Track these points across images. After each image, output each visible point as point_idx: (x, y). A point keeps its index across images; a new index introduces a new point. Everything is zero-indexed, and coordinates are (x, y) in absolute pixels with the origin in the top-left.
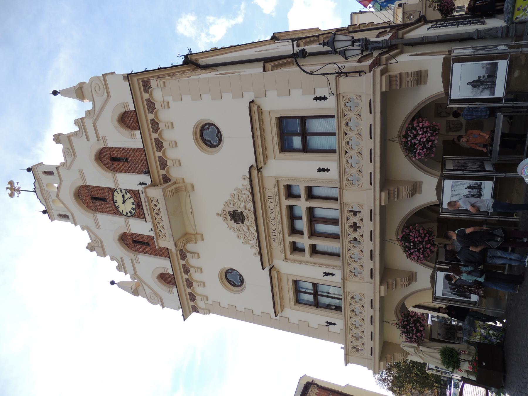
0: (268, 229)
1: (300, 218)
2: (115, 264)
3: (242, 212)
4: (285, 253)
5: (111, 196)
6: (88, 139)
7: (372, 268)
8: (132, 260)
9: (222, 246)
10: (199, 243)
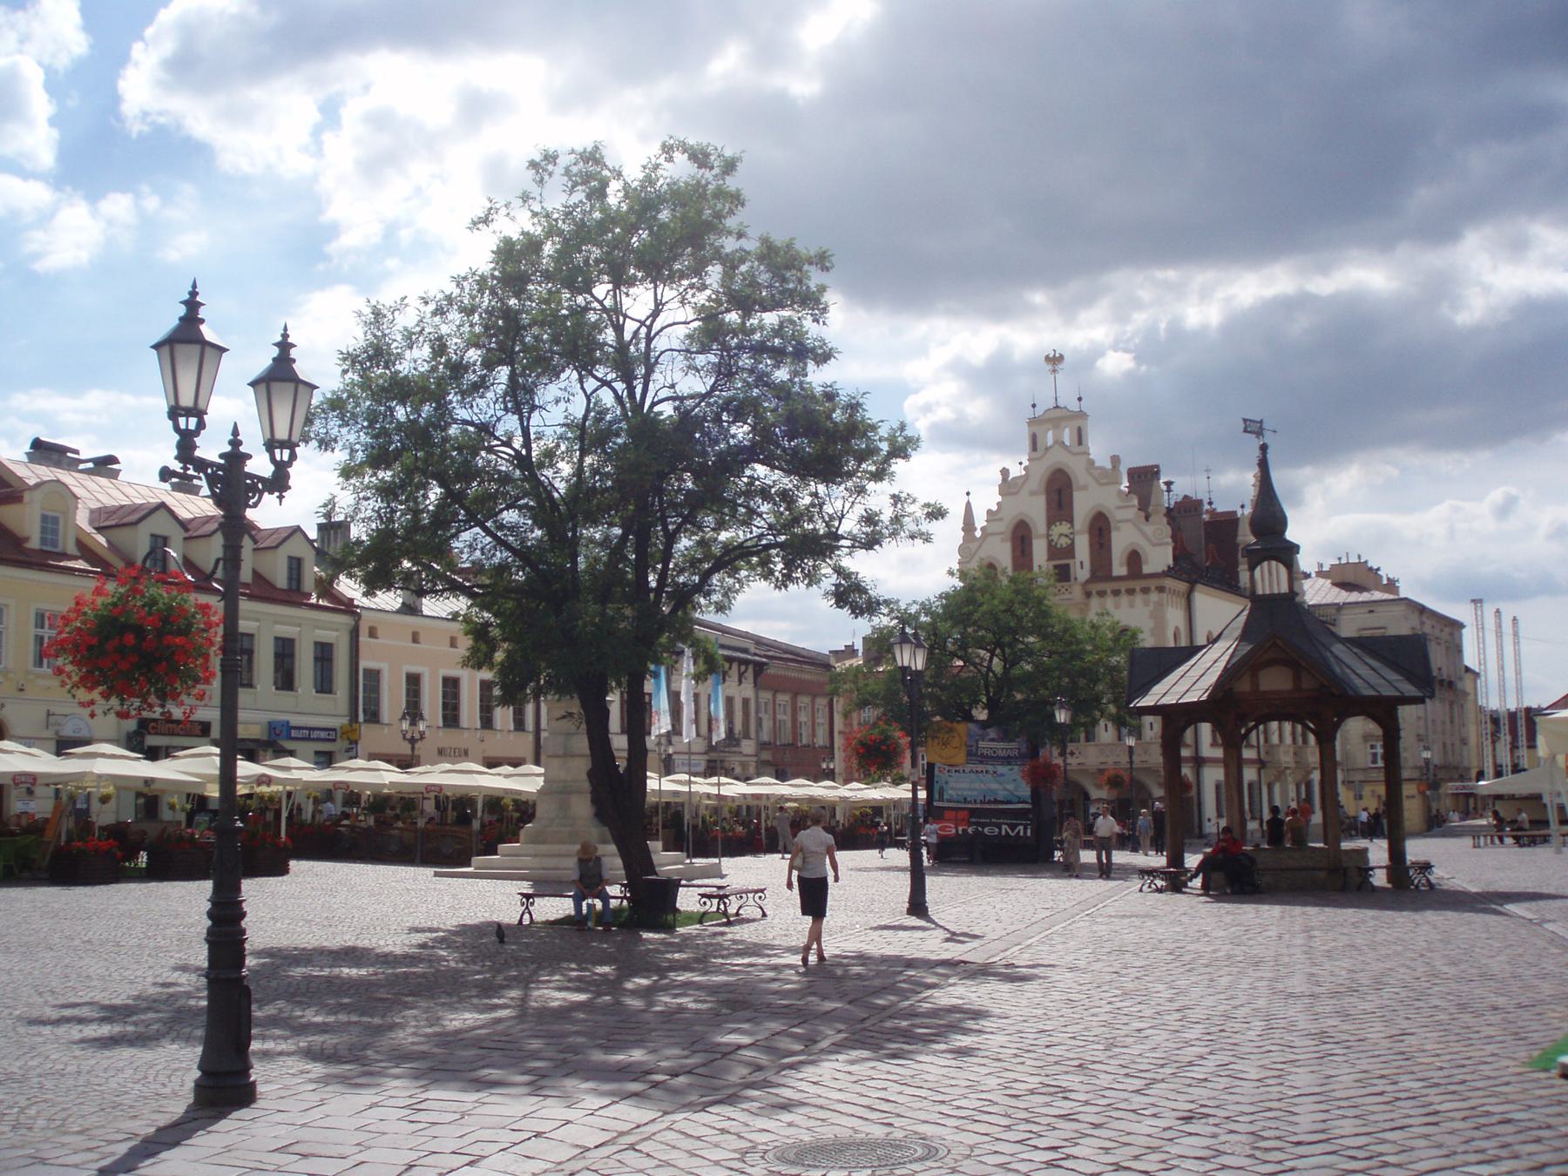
2: (995, 508)
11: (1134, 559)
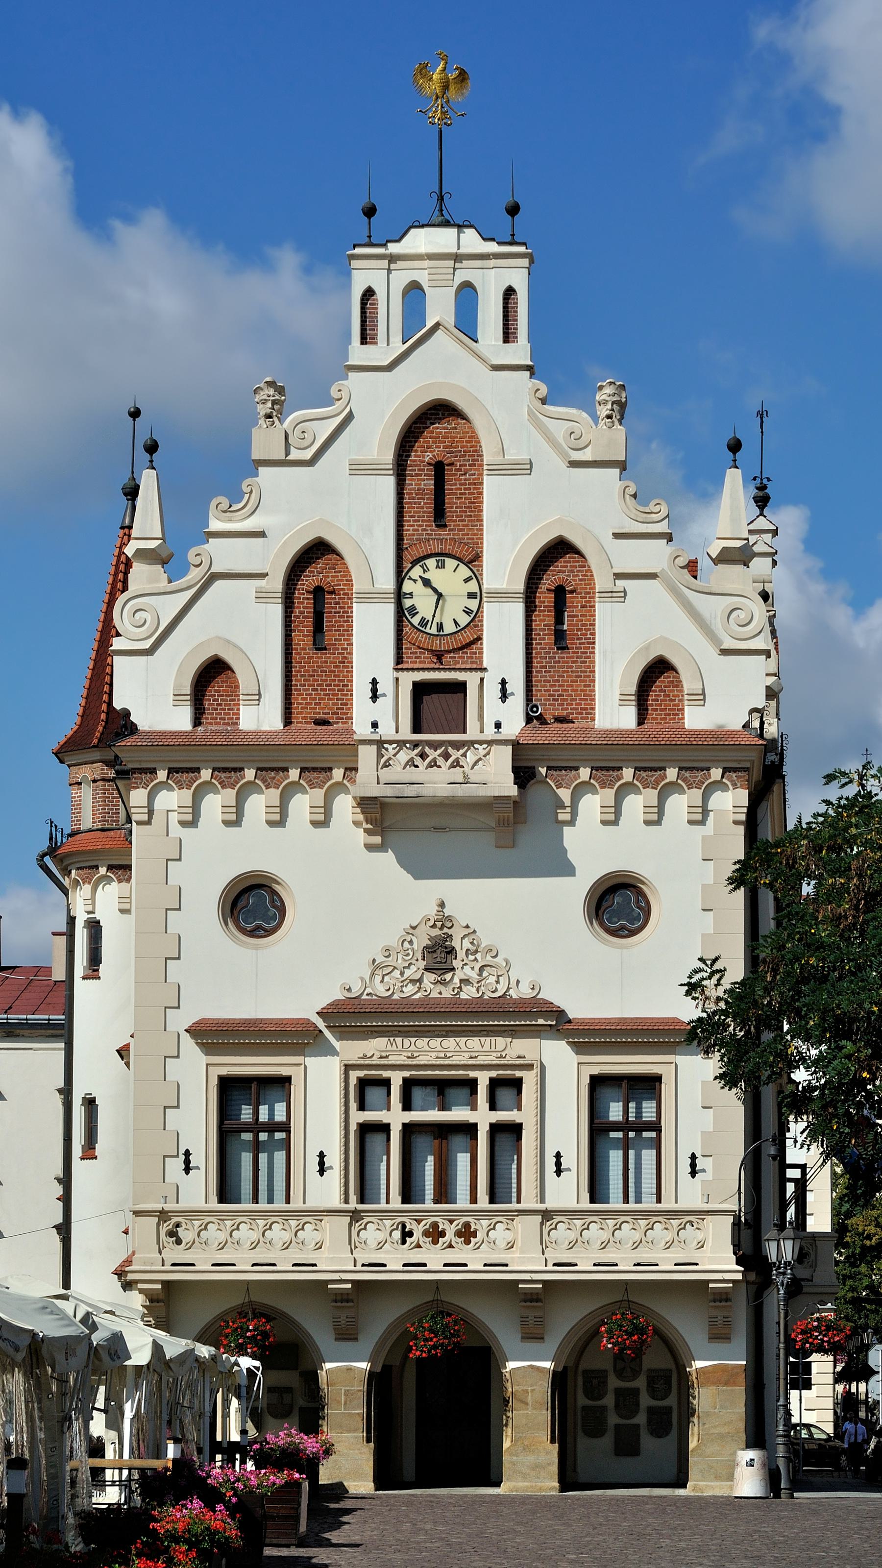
5: (457, 551)
6: (617, 536)
8: (263, 576)
10: (360, 836)
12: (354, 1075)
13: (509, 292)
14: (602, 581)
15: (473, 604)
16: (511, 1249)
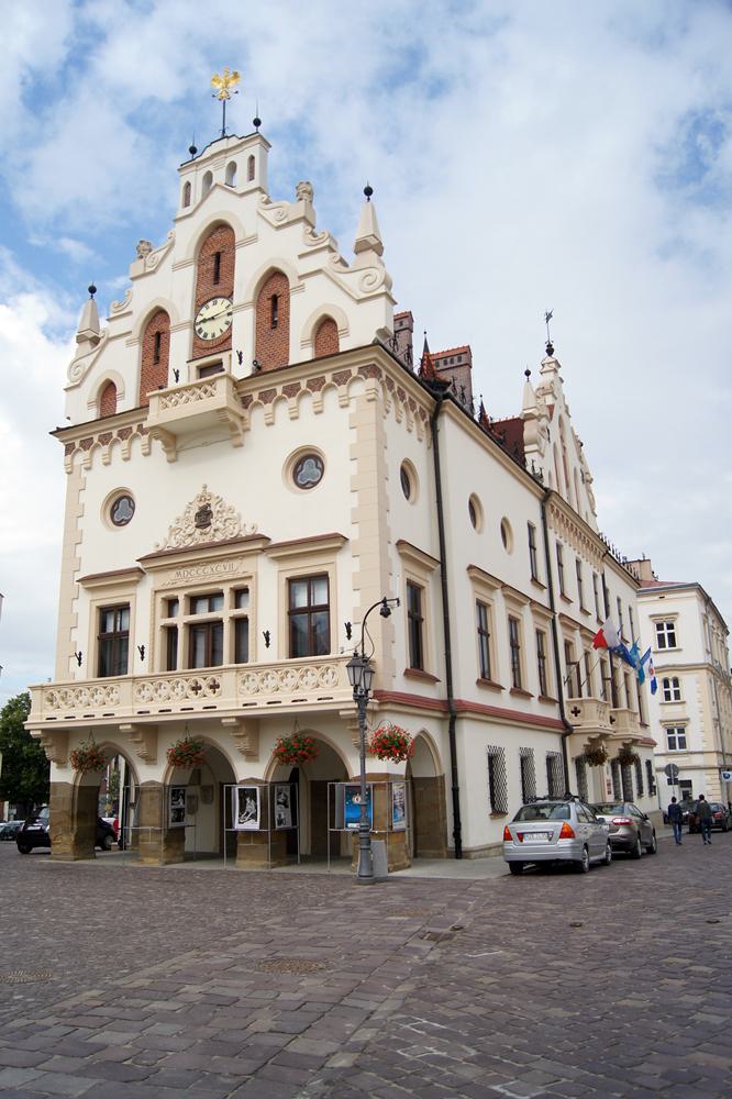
0: (191, 565)
1: (211, 609)
3: (210, 524)
4: (163, 591)
5: (222, 293)
6: (301, 256)
7: (152, 713)
8: (130, 333)
9: (165, 495)
11: (326, 326)
12: (160, 596)
13: (252, 158)
14: (293, 282)
15: (229, 319)
16: (232, 694)
